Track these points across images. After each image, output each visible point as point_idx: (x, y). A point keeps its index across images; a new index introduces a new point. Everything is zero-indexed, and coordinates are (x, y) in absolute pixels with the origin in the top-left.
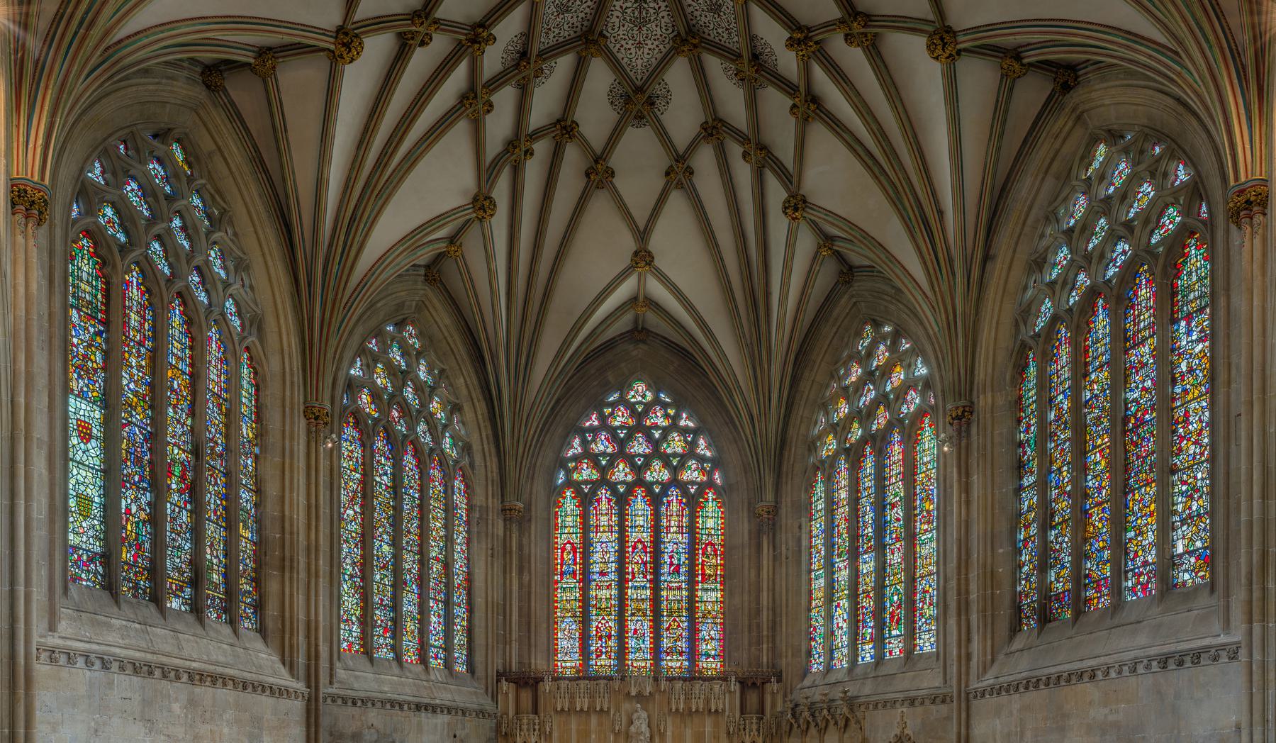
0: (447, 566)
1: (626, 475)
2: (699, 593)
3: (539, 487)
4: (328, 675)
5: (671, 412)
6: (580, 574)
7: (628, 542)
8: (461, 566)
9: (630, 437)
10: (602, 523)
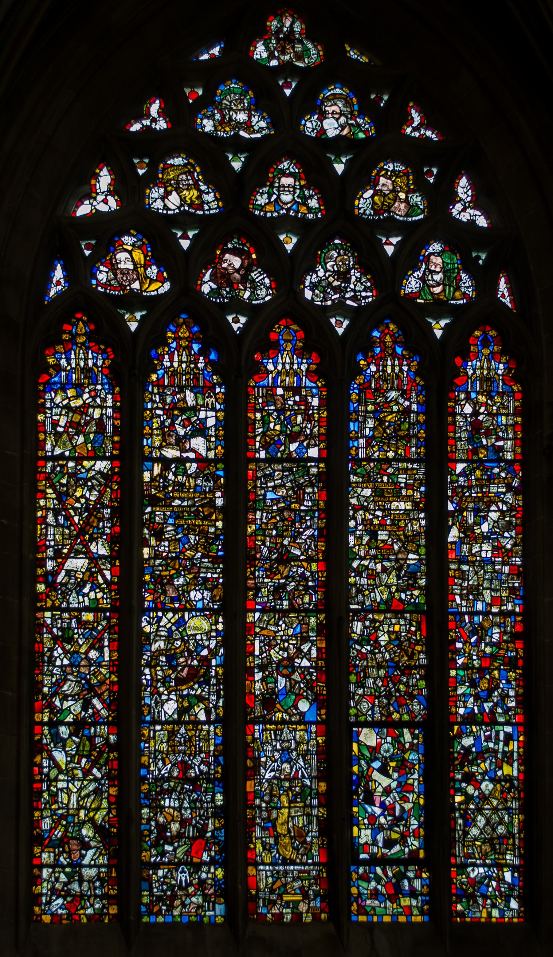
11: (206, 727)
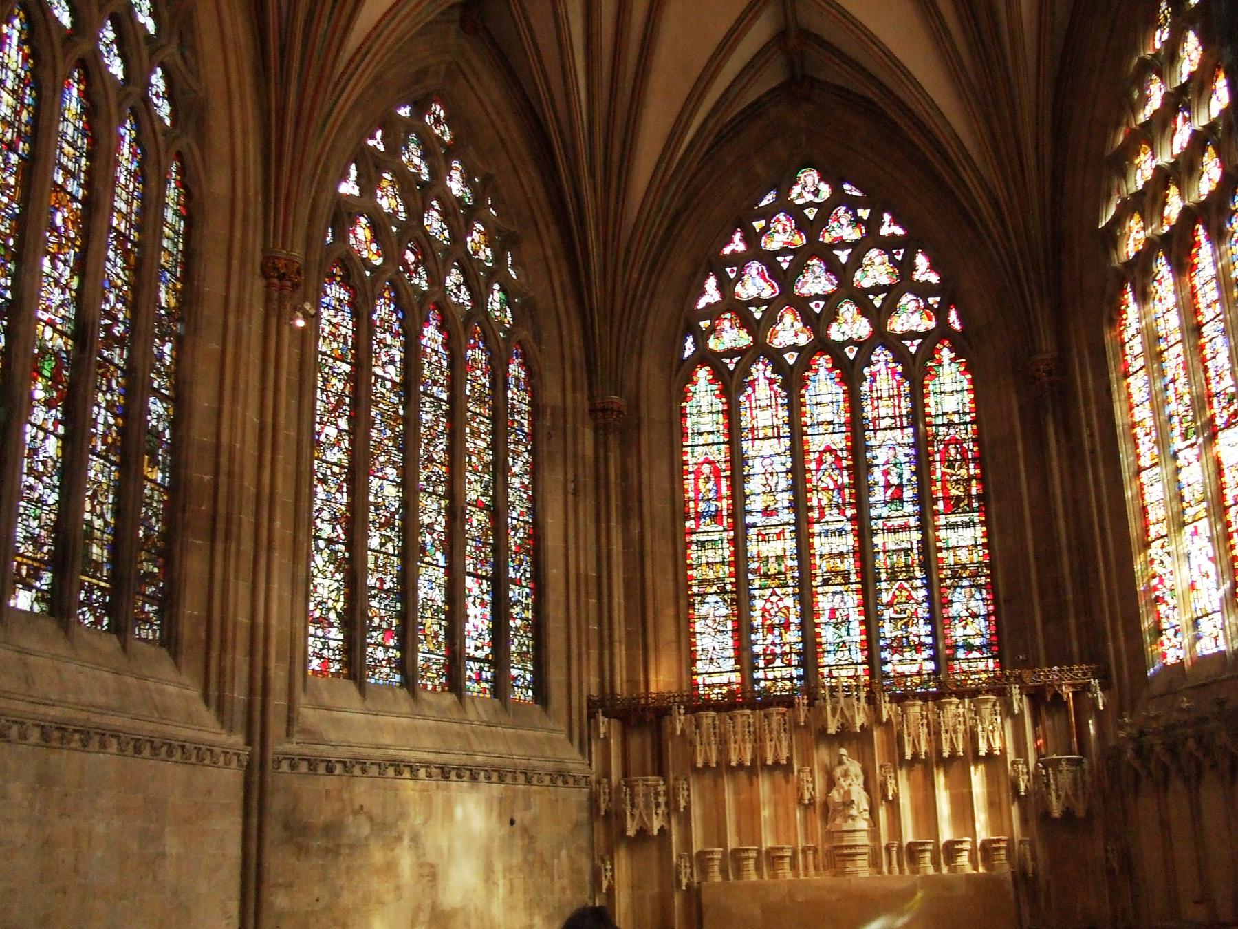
0: (497, 512)
1: (796, 335)
2: (942, 534)
3: (652, 369)
4: (285, 719)
5: (864, 213)
6: (729, 516)
7: (808, 452)
8: (522, 514)
9: (799, 267)
10: (761, 424)
11: (393, 558)
